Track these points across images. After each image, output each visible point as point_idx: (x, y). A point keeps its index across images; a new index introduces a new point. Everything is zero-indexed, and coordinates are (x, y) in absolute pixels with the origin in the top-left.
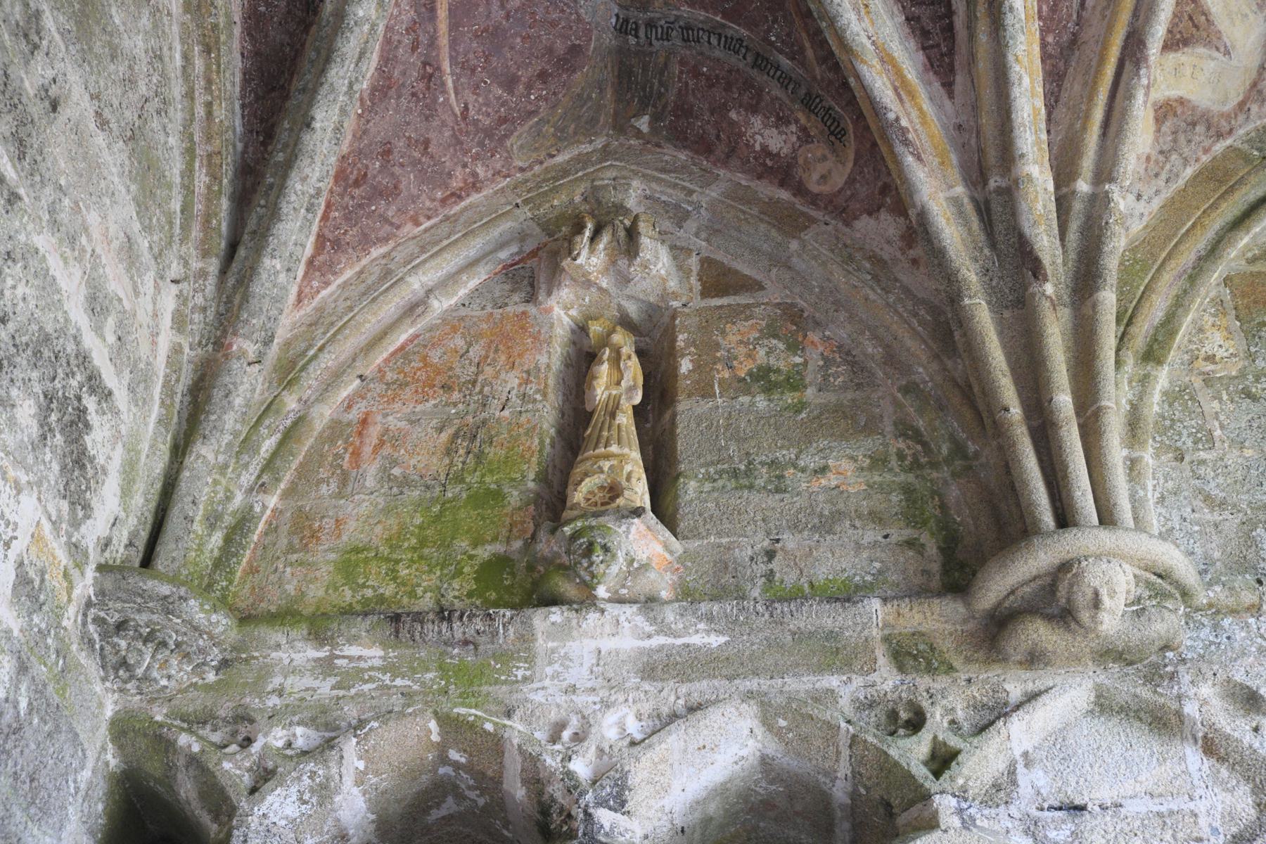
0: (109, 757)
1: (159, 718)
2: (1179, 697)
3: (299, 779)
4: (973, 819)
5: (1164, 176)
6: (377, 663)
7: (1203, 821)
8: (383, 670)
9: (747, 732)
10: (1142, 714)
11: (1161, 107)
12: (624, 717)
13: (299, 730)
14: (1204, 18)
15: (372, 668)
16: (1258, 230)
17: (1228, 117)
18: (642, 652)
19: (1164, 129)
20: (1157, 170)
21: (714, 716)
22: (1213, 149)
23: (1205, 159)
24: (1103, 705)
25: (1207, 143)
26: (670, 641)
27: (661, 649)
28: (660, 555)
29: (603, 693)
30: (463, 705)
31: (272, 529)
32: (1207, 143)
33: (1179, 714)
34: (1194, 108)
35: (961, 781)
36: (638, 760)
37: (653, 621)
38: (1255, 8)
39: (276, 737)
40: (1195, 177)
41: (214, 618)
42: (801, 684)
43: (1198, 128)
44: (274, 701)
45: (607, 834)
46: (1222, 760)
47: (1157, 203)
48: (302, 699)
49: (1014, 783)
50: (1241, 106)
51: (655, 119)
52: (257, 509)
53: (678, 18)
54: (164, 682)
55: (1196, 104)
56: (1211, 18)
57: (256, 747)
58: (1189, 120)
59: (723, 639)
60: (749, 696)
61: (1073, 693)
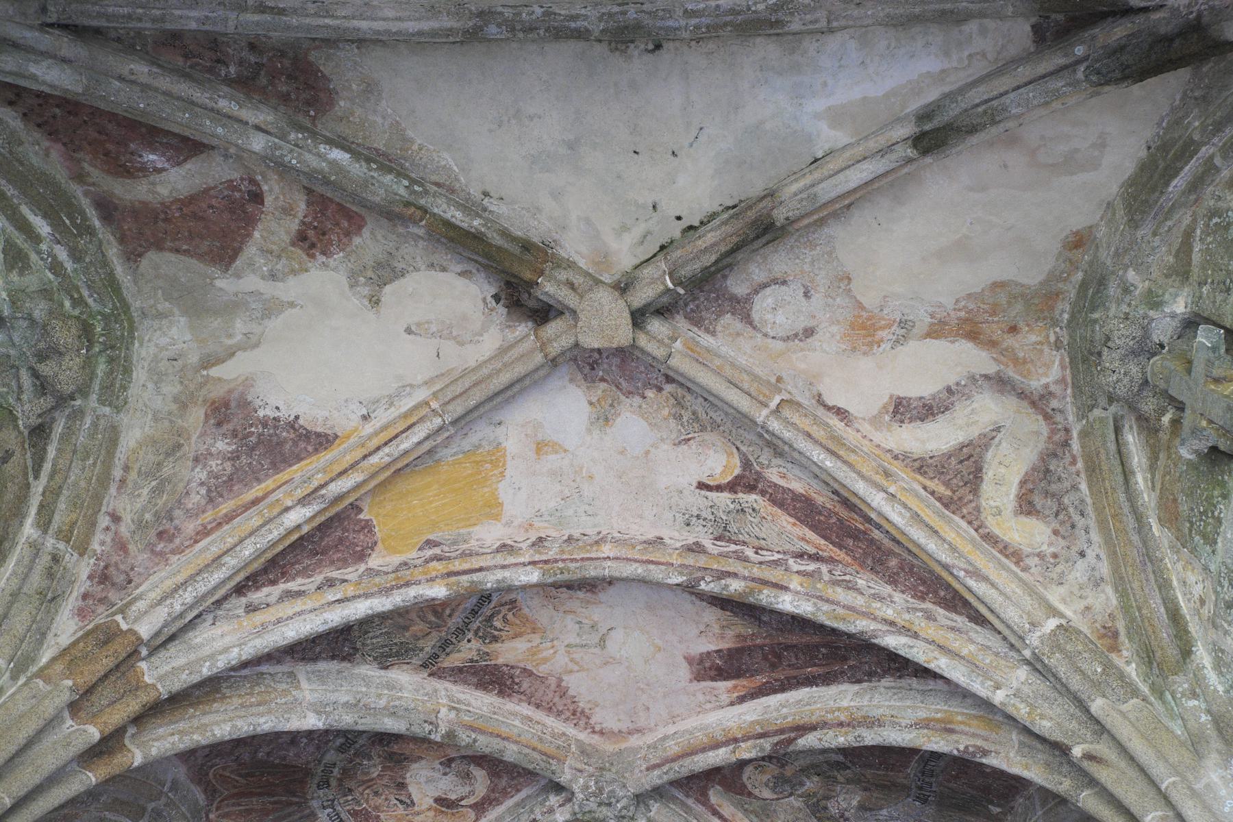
5: (1076, 518)
11: (1020, 506)
14: (964, 449)
16: (1136, 459)
17: (1053, 432)
19: (1039, 507)
20: (1068, 525)
22: (1075, 452)
23: (1080, 465)
25: (1068, 459)
32: (1068, 459)
34: (1034, 469)
38: (968, 402)
40: (1090, 488)
43: (1052, 468)
47: (1095, 536)
50: (1047, 417)
51: (992, 803)
53: (915, 775)
55: (1031, 466)
56: (967, 442)
58: (1041, 476)
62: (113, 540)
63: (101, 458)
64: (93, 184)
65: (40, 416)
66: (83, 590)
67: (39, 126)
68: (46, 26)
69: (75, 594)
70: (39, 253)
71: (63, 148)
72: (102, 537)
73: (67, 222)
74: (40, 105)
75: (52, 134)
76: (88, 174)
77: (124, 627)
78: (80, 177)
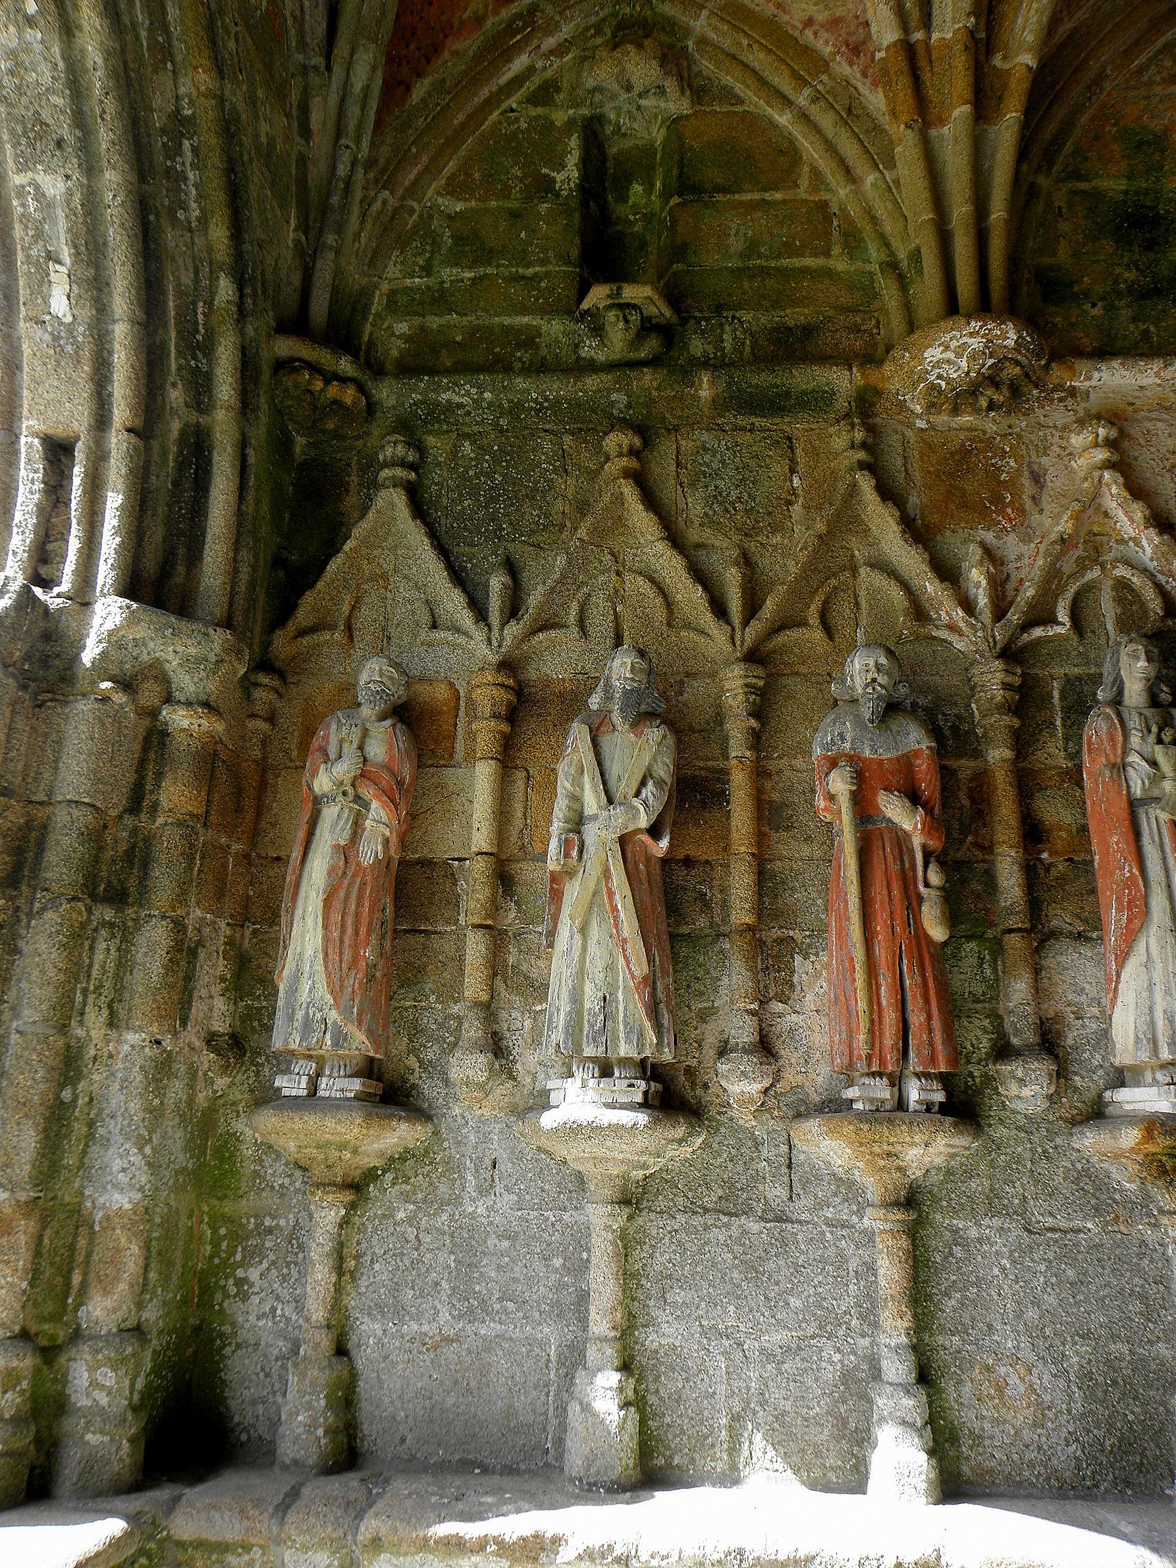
62: (827, 31)
63: (746, 29)
64: (486, 7)
65: (683, 93)
66: (859, 75)
67: (428, 62)
68: (329, 68)
69: (859, 85)
70: (545, 68)
71: (450, 38)
72: (821, 42)
73: (519, 37)
74: (408, 62)
75: (436, 50)
76: (476, 12)
77: (882, 54)
78: (479, 20)
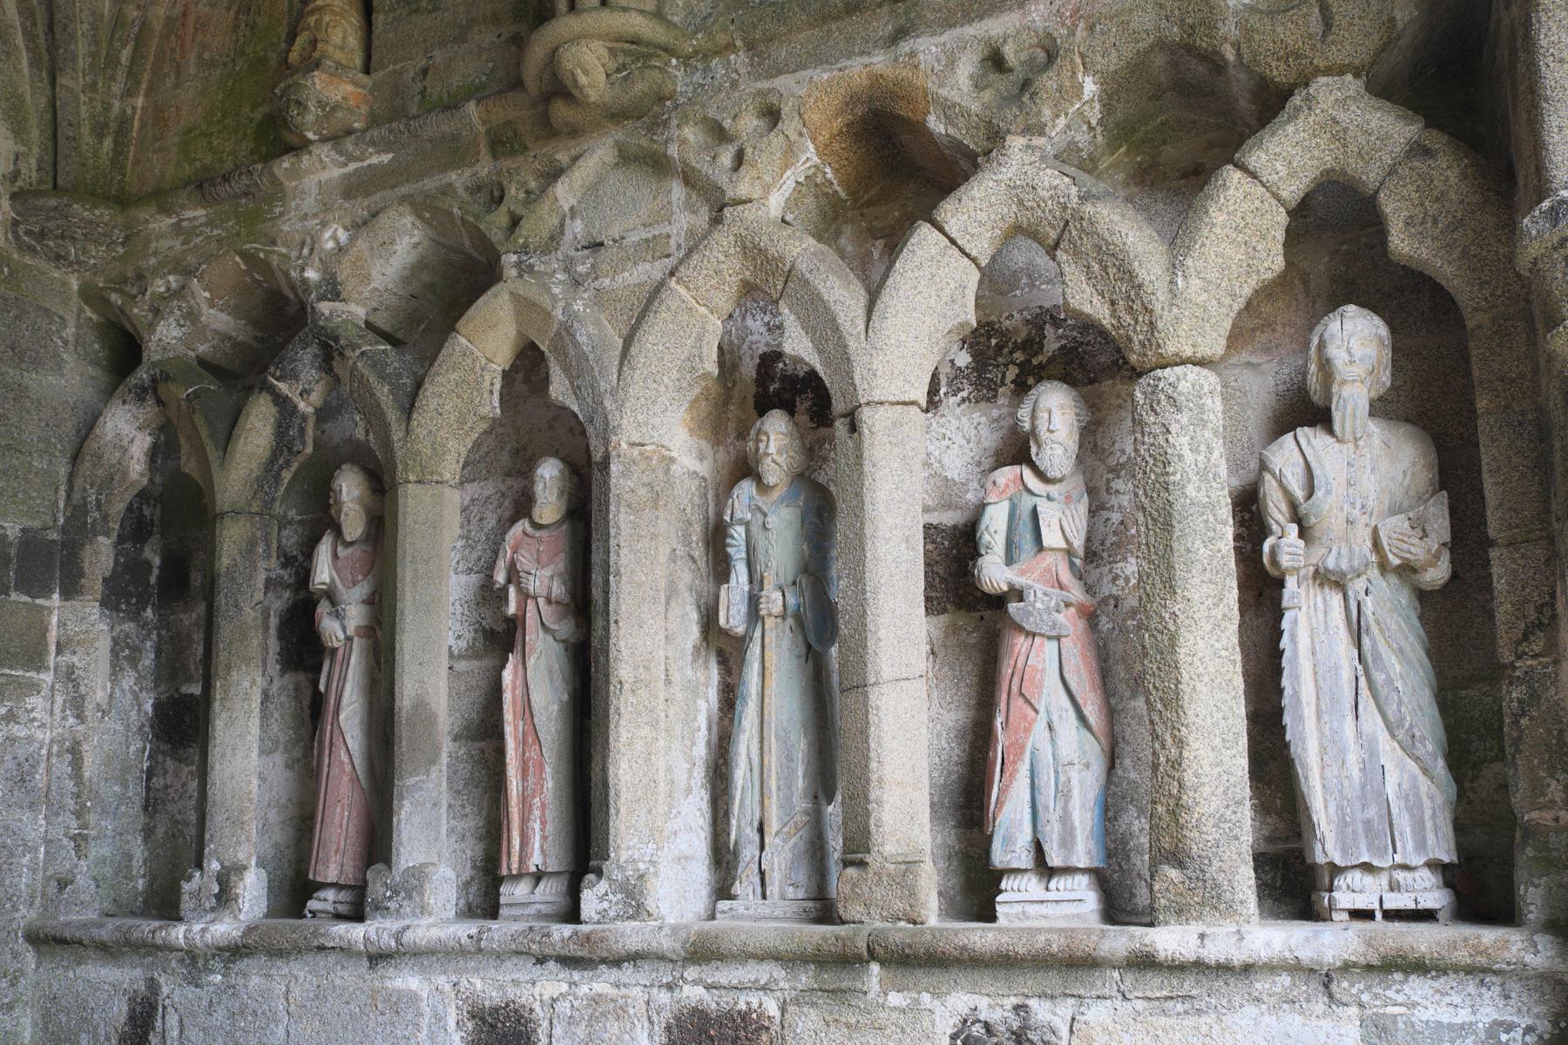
0: (89, 314)
1: (101, 285)
2: (666, 141)
3: (172, 312)
4: (531, 267)
6: (203, 220)
7: (672, 242)
8: (206, 225)
9: (409, 226)
10: (648, 161)
12: (336, 230)
13: (171, 278)
15: (201, 225)
18: (347, 177)
21: (384, 220)
24: (625, 158)
26: (360, 164)
27: (356, 170)
28: (352, 93)
29: (321, 216)
30: (248, 242)
31: (143, 125)
33: (665, 155)
35: (521, 241)
36: (340, 262)
37: (341, 153)
39: (159, 286)
41: (97, 212)
42: (430, 184)
44: (153, 261)
45: (327, 319)
46: (693, 187)
48: (167, 256)
49: (562, 233)
52: (129, 112)
54: (92, 261)
57: (148, 293)
59: (390, 156)
60: (403, 200)
61: (599, 152)
